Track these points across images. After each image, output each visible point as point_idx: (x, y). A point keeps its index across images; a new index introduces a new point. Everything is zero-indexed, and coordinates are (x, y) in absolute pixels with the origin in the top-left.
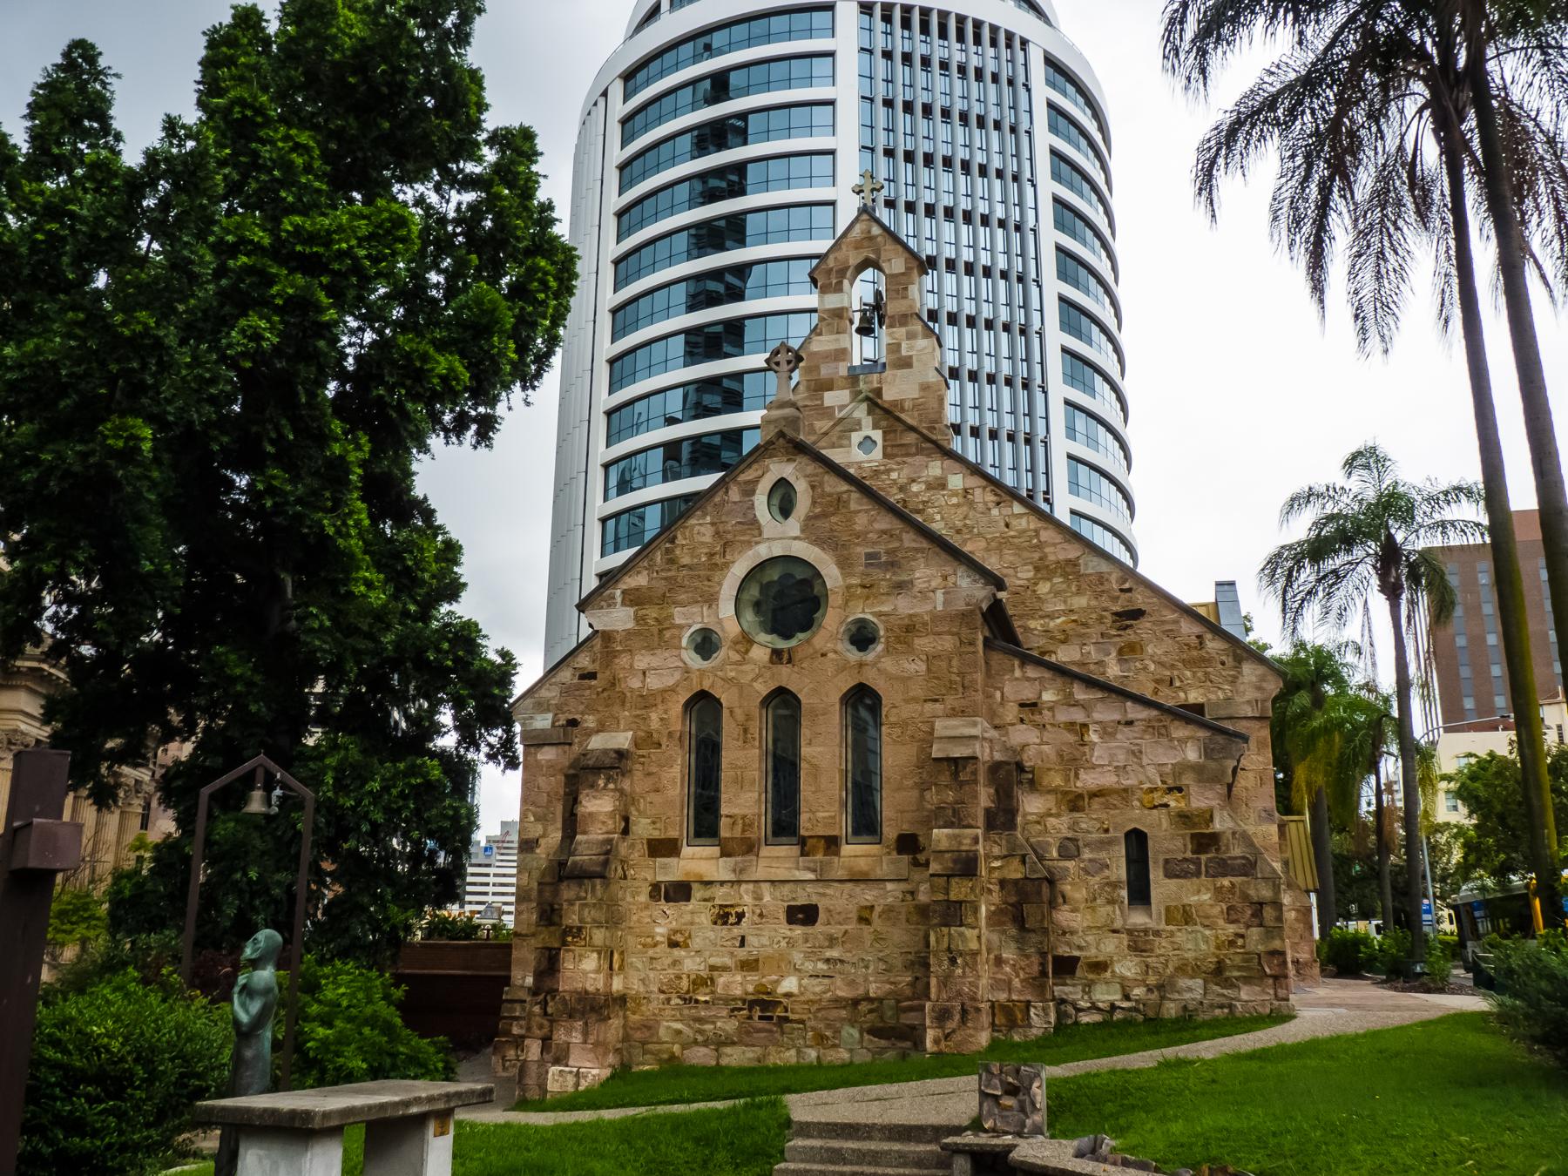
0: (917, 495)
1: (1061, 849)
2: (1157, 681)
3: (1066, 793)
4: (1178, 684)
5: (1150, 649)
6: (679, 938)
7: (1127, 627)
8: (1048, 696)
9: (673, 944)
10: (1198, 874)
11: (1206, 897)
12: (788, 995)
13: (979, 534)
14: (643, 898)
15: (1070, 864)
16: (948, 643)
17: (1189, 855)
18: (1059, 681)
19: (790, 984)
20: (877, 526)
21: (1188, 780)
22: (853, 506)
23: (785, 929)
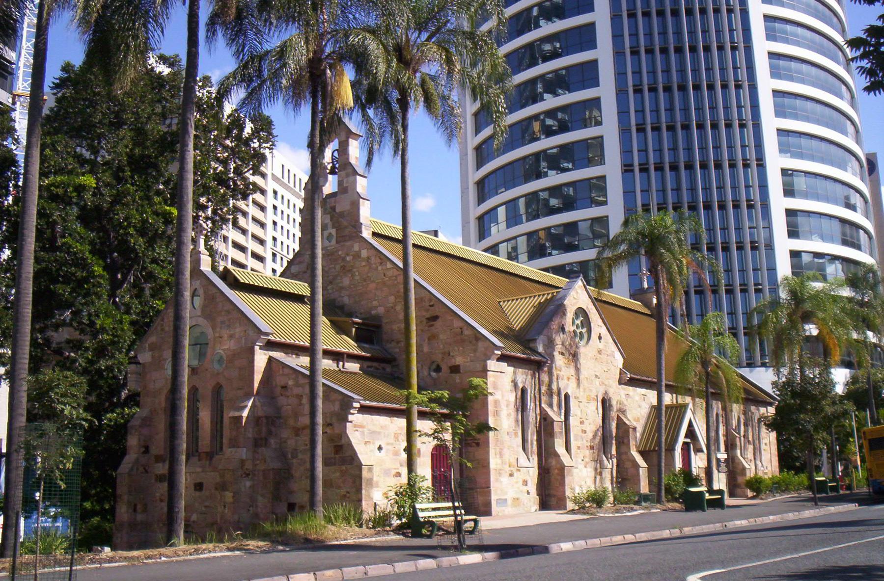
0: (349, 262)
1: (292, 453)
2: (444, 353)
3: (294, 428)
4: (452, 354)
5: (441, 336)
7: (432, 325)
8: (290, 383)
10: (335, 464)
11: (338, 474)
12: (194, 522)
13: (373, 282)
14: (153, 481)
15: (294, 461)
17: (333, 455)
18: (294, 376)
20: (225, 308)
21: (334, 420)
22: (218, 300)
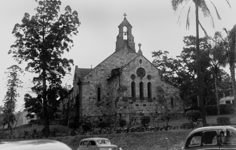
6: (132, 108)
9: (132, 108)
16: (157, 79)
19: (144, 112)
23: (143, 107)
